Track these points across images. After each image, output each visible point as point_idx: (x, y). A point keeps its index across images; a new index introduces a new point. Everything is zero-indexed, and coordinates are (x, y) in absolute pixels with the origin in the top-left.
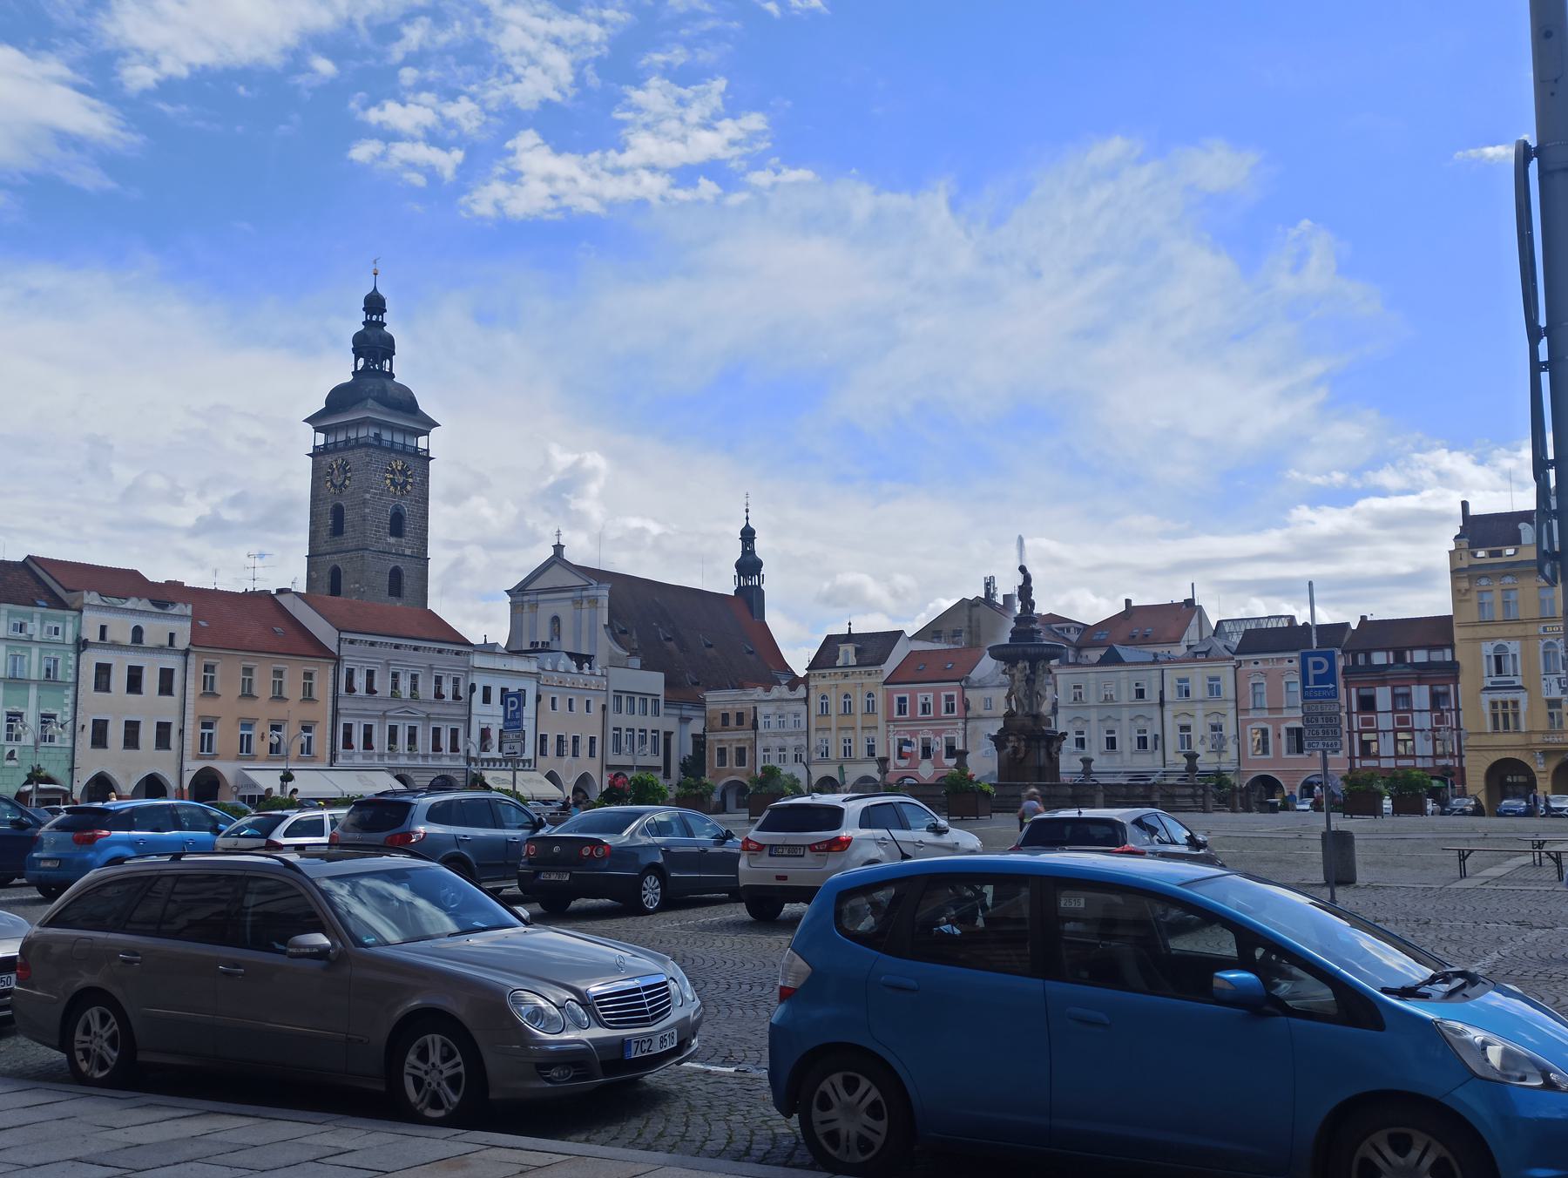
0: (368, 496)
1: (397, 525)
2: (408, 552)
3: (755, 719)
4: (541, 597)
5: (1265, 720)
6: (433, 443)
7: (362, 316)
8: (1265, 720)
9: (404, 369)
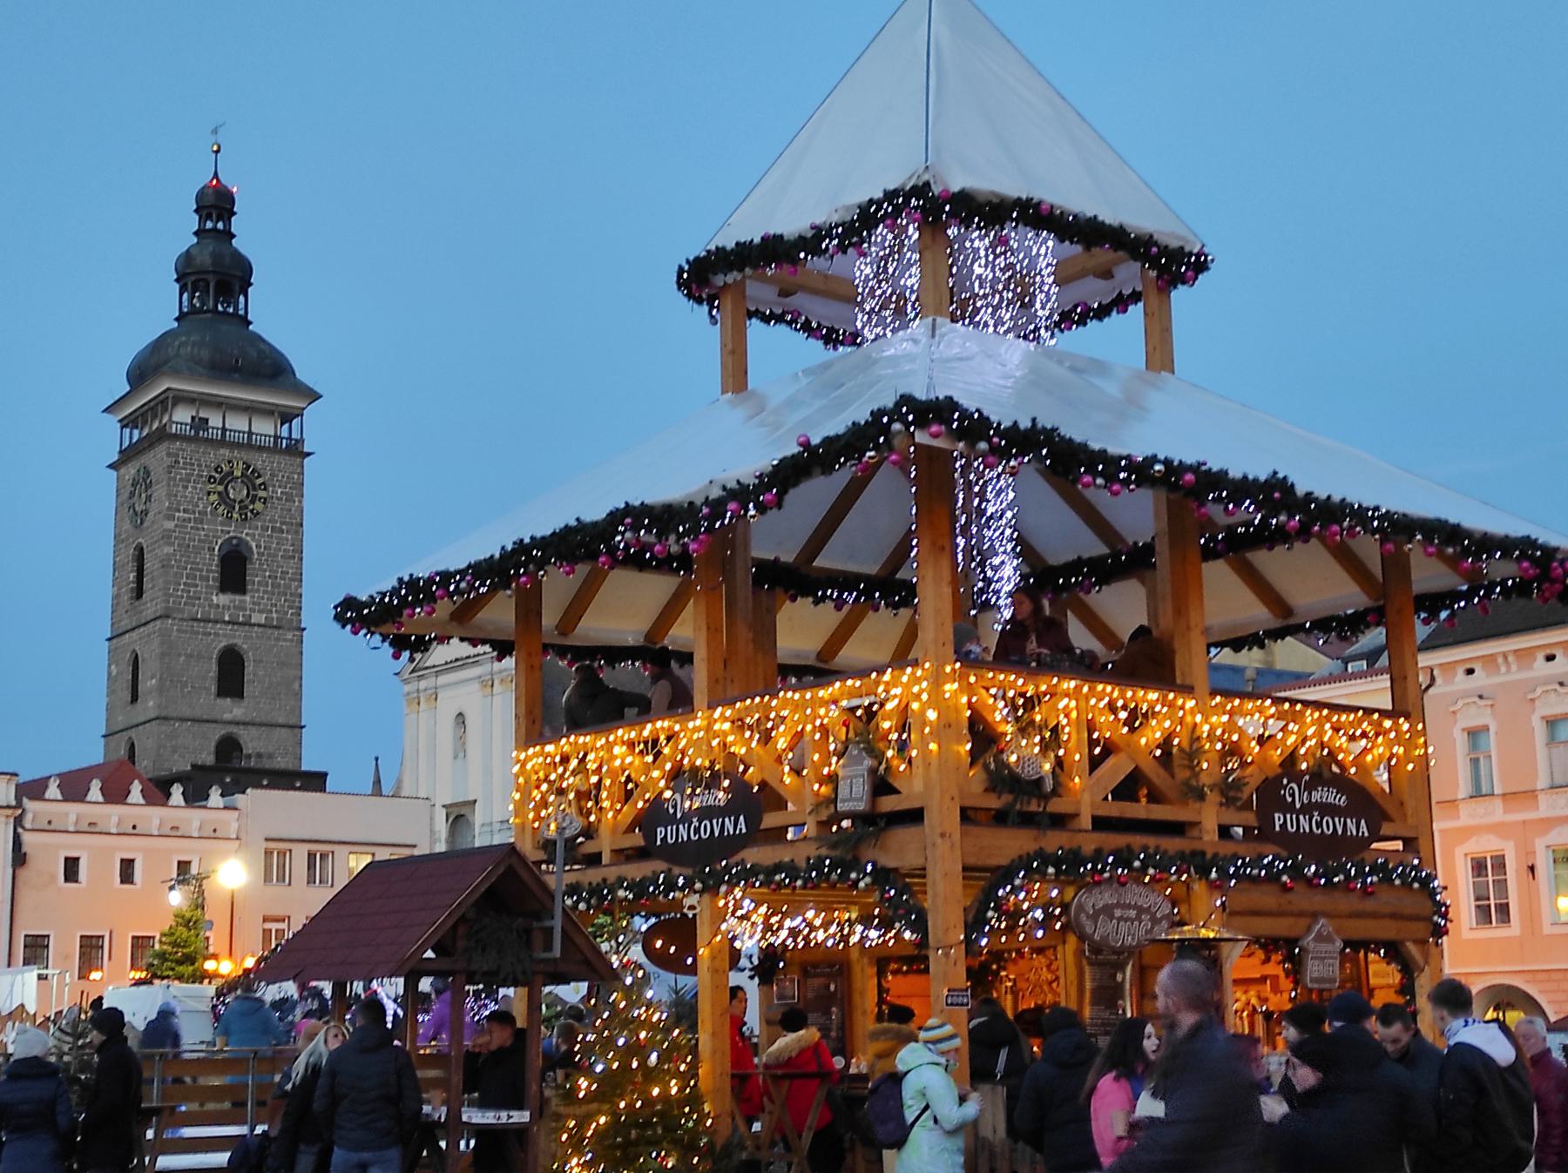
0: (170, 525)
1: (234, 571)
4: (443, 679)
5: (1498, 829)
6: (314, 426)
7: (194, 222)
8: (1498, 829)
9: (269, 312)
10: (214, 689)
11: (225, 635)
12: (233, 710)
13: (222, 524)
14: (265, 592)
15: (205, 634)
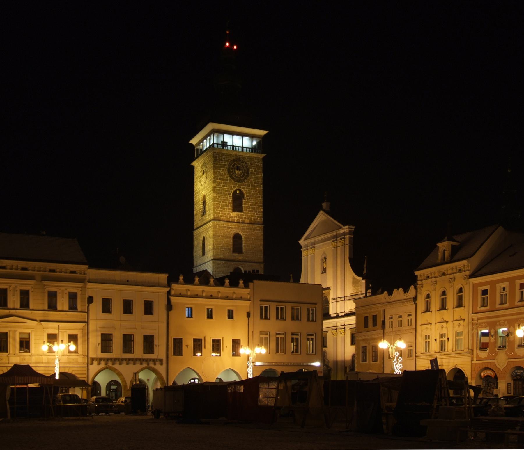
3: (384, 323)
11: (235, 228)
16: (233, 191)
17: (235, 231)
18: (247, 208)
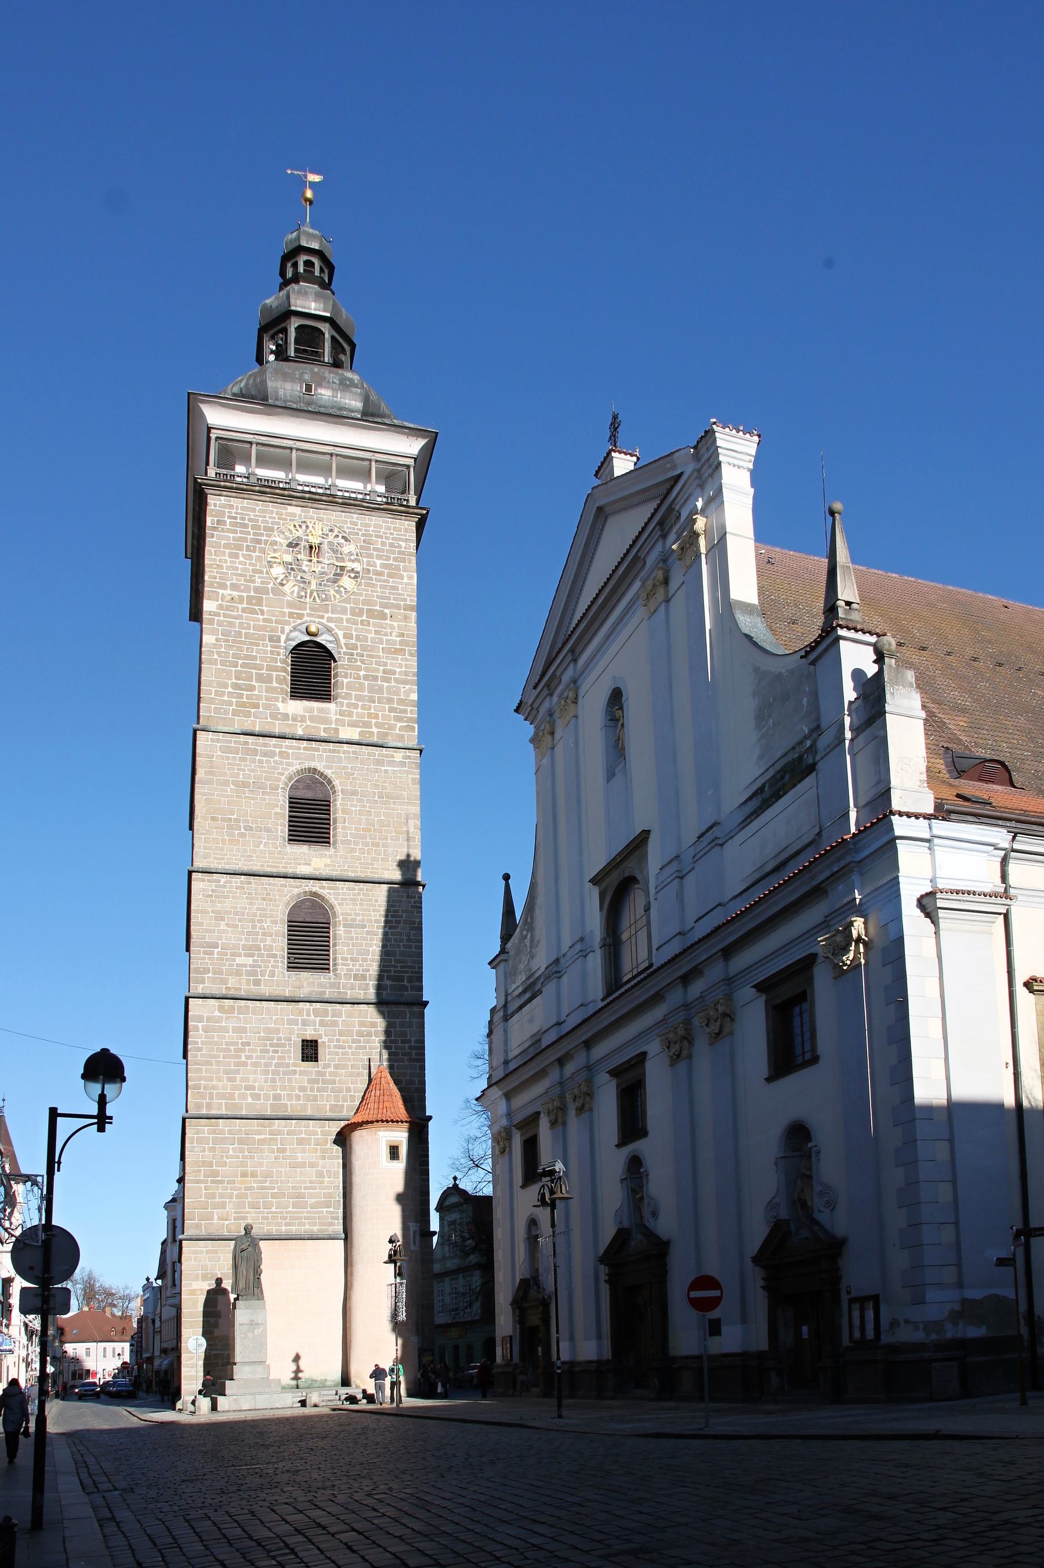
2: (346, 733)
10: (283, 828)
11: (297, 757)
12: (311, 859)
13: (290, 605)
14: (359, 698)
15: (265, 755)
16: (287, 629)
17: (296, 766)
18: (350, 686)
